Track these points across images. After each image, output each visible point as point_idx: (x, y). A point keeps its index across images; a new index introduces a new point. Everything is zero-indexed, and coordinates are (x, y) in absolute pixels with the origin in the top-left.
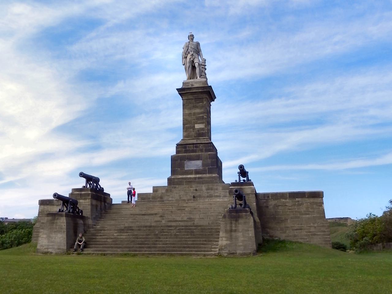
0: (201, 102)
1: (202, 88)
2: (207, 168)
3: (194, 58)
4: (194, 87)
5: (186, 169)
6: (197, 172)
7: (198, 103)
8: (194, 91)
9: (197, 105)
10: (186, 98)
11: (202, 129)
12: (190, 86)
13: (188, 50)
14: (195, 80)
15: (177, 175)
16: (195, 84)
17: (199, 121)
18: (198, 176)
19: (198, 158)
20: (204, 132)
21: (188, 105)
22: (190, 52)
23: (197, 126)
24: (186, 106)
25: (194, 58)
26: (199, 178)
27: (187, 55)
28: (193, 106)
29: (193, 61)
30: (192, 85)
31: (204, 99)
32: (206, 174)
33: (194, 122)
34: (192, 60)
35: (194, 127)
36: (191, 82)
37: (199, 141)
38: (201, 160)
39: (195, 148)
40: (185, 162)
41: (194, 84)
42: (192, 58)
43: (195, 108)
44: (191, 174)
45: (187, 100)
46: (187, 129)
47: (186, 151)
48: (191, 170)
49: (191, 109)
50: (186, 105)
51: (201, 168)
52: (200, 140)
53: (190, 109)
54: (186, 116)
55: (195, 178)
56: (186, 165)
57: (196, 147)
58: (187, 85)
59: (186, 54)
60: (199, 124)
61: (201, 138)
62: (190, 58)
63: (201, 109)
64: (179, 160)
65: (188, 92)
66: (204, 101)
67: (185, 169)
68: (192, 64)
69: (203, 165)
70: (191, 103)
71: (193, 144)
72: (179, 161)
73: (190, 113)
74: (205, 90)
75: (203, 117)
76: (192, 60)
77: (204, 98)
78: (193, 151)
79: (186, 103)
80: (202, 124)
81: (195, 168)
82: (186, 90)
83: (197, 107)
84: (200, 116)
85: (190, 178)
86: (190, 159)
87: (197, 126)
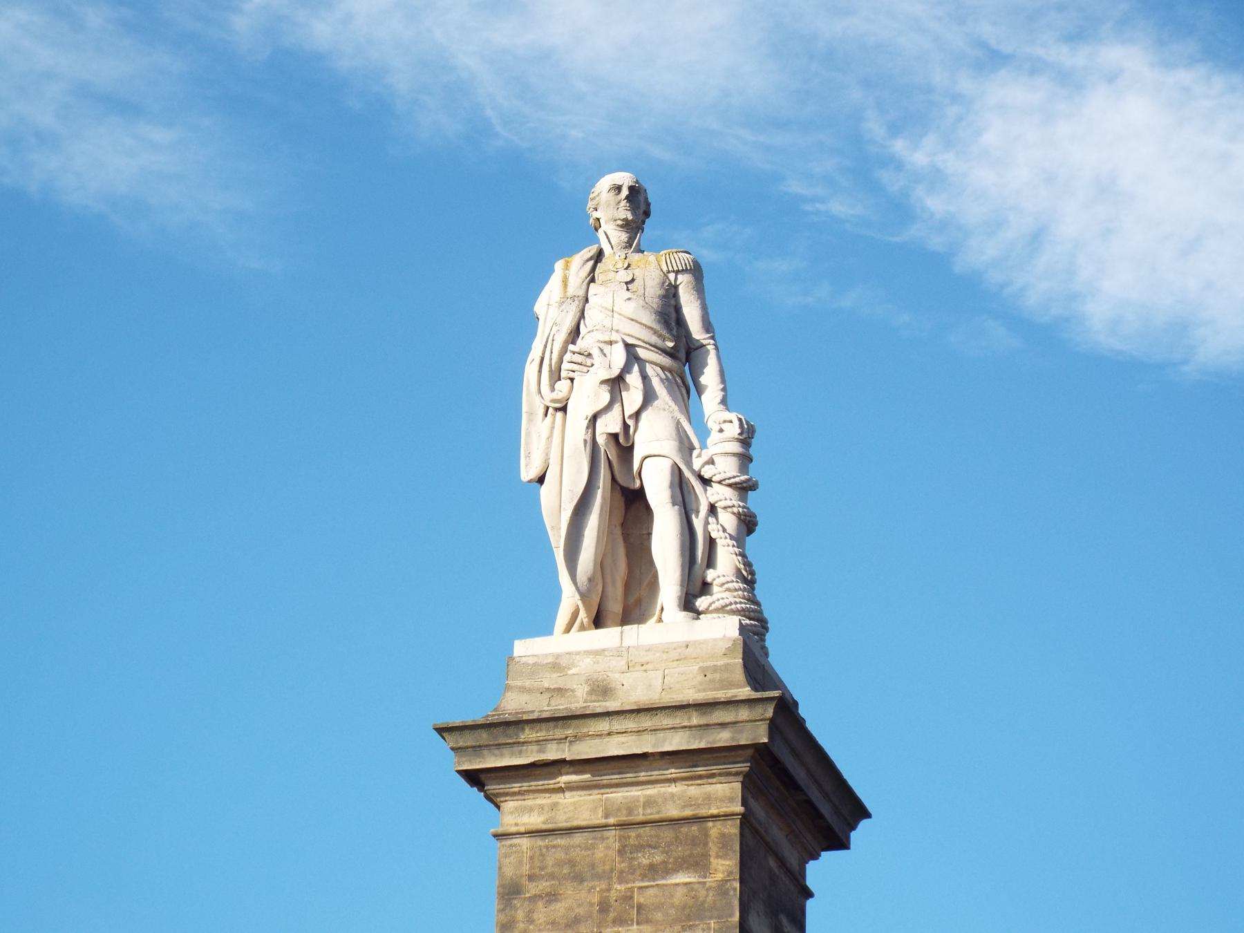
0: (684, 864)
1: (696, 719)
3: (637, 415)
4: (612, 705)
7: (653, 871)
9: (638, 898)
10: (535, 820)
12: (579, 700)
13: (575, 333)
14: (634, 635)
16: (628, 679)
21: (552, 897)
24: (534, 899)
25: (637, 415)
27: (563, 385)
28: (604, 907)
29: (623, 446)
30: (602, 689)
31: (714, 829)
34: (616, 428)
36: (588, 653)
41: (616, 678)
42: (617, 407)
45: (540, 842)
50: (533, 889)
58: (550, 680)
59: (556, 376)
62: (595, 418)
65: (552, 754)
66: (713, 849)
68: (613, 479)
70: (579, 878)
74: (723, 738)
76: (616, 428)
77: (714, 817)
79: (531, 878)
82: (528, 734)
83: (640, 907)
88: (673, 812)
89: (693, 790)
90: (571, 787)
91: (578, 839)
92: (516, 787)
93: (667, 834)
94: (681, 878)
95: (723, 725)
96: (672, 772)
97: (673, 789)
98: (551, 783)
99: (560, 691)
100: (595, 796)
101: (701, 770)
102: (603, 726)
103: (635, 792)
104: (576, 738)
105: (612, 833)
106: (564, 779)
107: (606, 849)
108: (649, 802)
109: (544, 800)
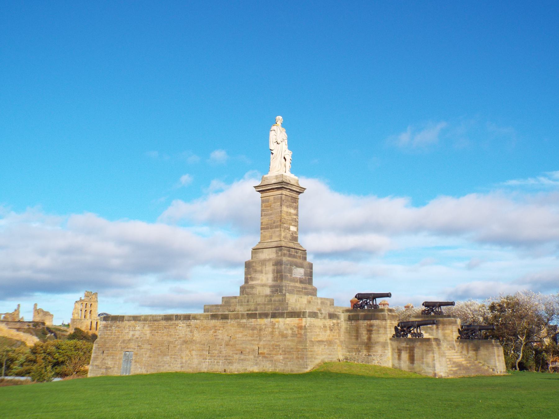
2: (307, 277)
5: (293, 276)
6: (301, 282)
7: (293, 203)
8: (294, 189)
11: (295, 233)
12: (288, 182)
15: (288, 281)
17: (293, 223)
18: (303, 285)
19: (301, 266)
20: (296, 236)
22: (285, 140)
23: (293, 229)
26: (305, 288)
30: (289, 181)
32: (306, 284)
33: (290, 223)
35: (289, 228)
37: (296, 246)
38: (304, 268)
39: (296, 254)
40: (293, 268)
41: (291, 181)
43: (291, 207)
44: (297, 282)
46: (285, 229)
47: (290, 256)
48: (297, 278)
49: (288, 208)
51: (304, 277)
52: (296, 245)
53: (287, 207)
54: (284, 214)
55: (303, 288)
56: (293, 272)
57: (297, 252)
58: (285, 178)
60: (293, 226)
61: (294, 242)
63: (295, 210)
64: (289, 265)
67: (293, 276)
69: (305, 274)
71: (294, 249)
72: (289, 267)
73: (287, 212)
75: (296, 219)
78: (294, 257)
80: (294, 227)
81: (300, 277)
82: (289, 185)
84: (294, 218)
85: (299, 288)
86: (298, 266)
87: (293, 229)
88: (294, 197)
89: (295, 195)
90: (288, 191)
91: (288, 197)
92: (285, 189)
93: (294, 199)
94: (295, 204)
95: (301, 190)
96: (295, 193)
97: (294, 194)
98: (286, 190)
99: (286, 180)
100: (289, 192)
101: (297, 193)
102: (294, 186)
103: (292, 194)
104: (292, 187)
105: (290, 197)
106: (288, 190)
107: (290, 199)
108: (292, 195)
109: (285, 191)
